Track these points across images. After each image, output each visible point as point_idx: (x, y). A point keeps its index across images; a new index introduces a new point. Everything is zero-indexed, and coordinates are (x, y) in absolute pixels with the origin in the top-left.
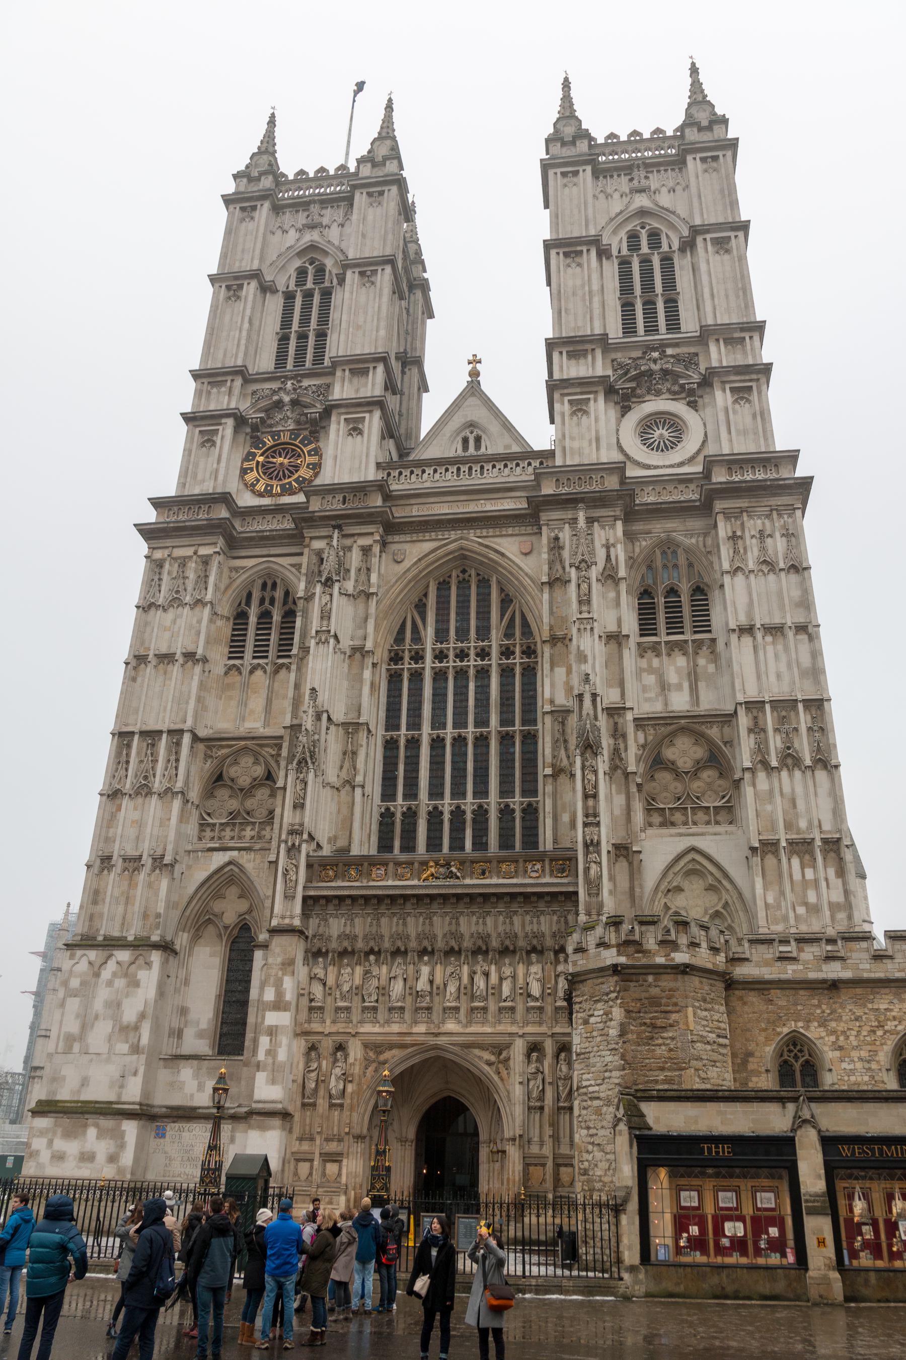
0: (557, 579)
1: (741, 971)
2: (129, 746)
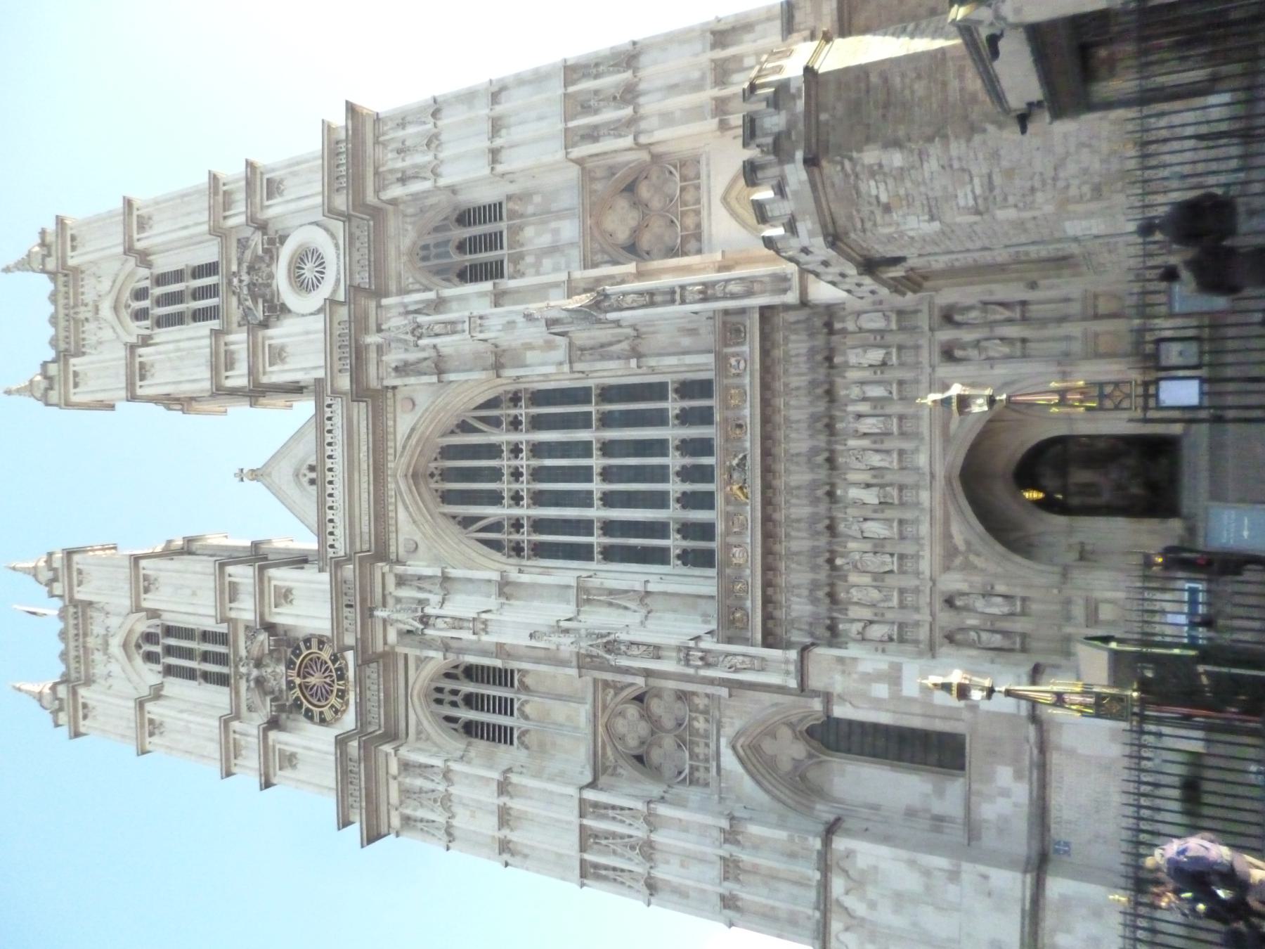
0: (437, 366)
2: (596, 866)
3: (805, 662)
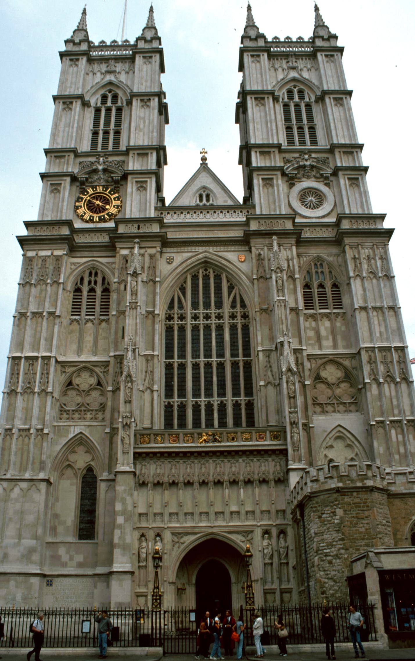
0: (261, 277)
1: (393, 488)
2: (18, 365)
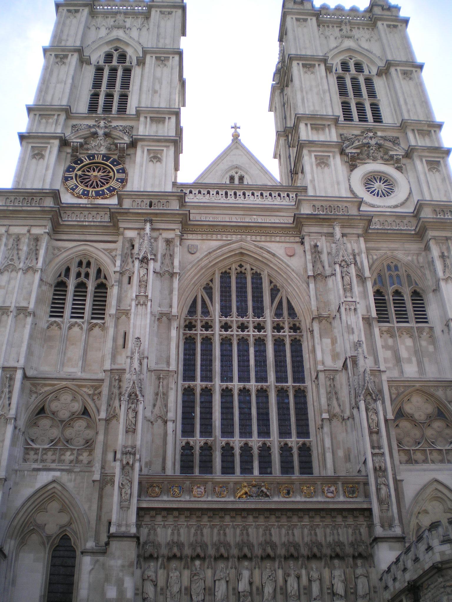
0: (319, 274)
3: (129, 539)
